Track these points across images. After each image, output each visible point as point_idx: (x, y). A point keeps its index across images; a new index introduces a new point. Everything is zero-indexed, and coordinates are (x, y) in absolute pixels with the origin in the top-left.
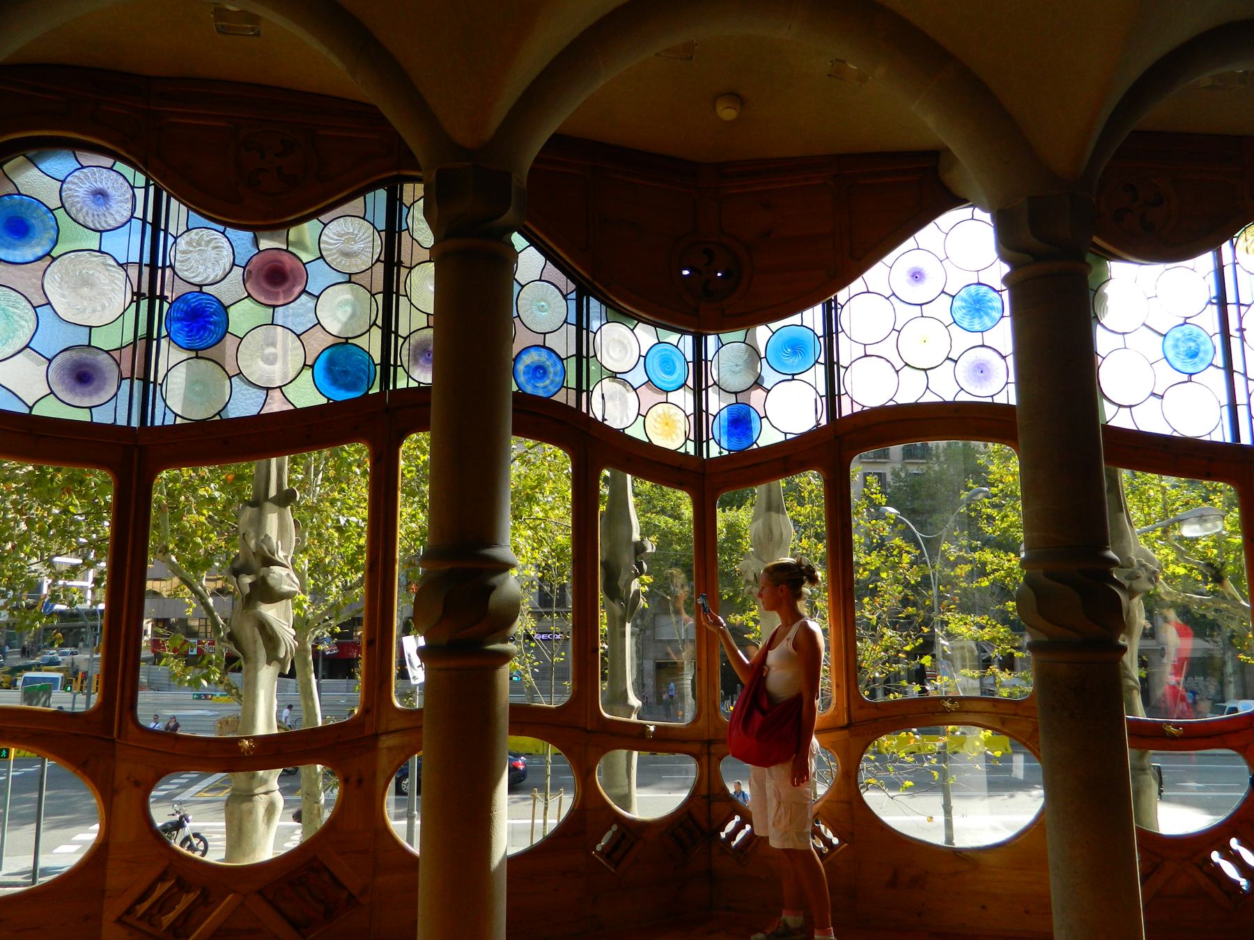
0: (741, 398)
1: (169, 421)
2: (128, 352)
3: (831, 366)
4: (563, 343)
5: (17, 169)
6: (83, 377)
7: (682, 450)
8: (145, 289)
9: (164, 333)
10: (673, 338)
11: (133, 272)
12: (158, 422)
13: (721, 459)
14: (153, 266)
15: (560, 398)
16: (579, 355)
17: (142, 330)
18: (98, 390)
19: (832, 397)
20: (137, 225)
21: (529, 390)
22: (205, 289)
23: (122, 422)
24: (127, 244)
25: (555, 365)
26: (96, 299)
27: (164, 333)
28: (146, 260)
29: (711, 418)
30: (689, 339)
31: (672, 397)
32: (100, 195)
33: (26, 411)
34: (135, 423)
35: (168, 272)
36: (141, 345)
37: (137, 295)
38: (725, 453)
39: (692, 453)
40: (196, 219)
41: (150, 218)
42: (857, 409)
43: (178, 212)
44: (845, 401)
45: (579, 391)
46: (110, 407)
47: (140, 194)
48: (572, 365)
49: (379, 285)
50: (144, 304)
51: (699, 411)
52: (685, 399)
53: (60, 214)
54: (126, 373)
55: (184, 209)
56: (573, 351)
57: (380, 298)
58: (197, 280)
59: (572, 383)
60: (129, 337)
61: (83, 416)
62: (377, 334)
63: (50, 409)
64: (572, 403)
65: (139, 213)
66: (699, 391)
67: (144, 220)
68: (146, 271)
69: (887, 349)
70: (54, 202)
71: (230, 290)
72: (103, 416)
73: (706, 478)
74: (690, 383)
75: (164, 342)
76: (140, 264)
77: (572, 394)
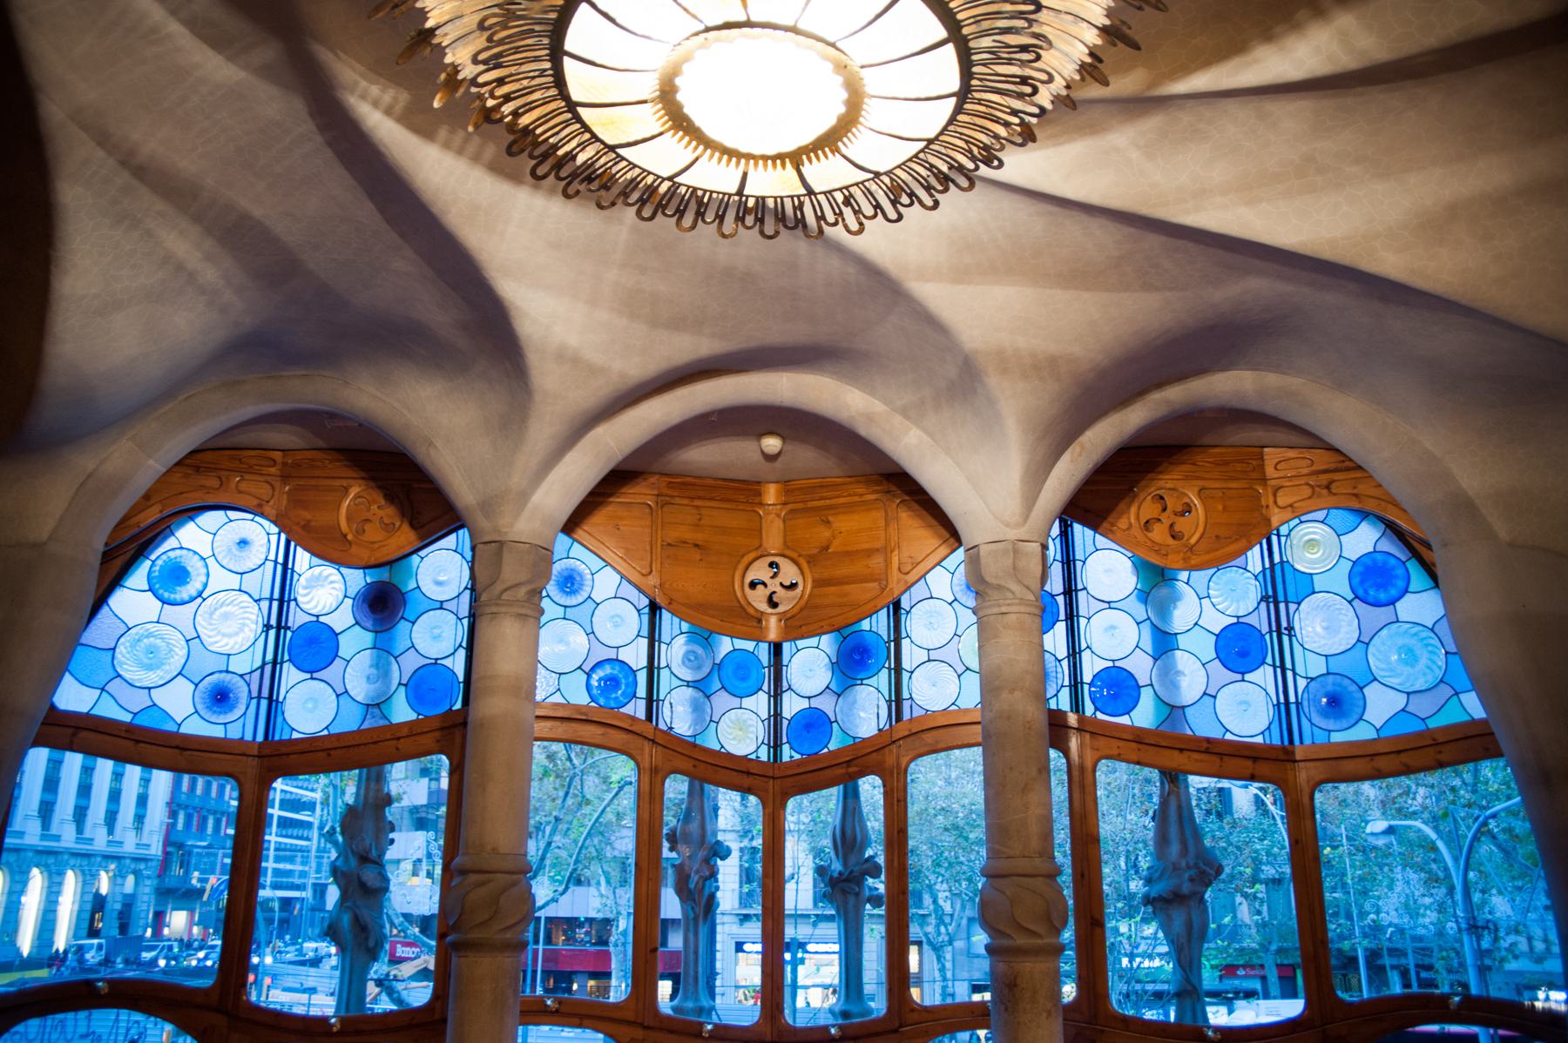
0: (815, 703)
1: (286, 737)
2: (257, 674)
3: (898, 669)
4: (636, 657)
5: (182, 524)
6: (221, 698)
7: (753, 757)
8: (273, 622)
9: (286, 657)
10: (749, 645)
11: (264, 605)
12: (277, 738)
13: (792, 763)
14: (281, 601)
15: (628, 710)
16: (652, 668)
17: (269, 657)
18: (232, 708)
19: (897, 701)
20: (270, 565)
21: (602, 701)
22: (322, 619)
23: (248, 737)
24: (263, 582)
25: (626, 677)
26: (234, 631)
27: (286, 657)
28: (276, 595)
29: (785, 723)
30: (764, 647)
31: (747, 702)
32: (243, 543)
33: (174, 729)
34: (260, 738)
35: (293, 604)
36: (268, 669)
37: (268, 627)
38: (797, 756)
39: (764, 758)
40: (316, 560)
41: (281, 560)
42: (917, 713)
43: (302, 558)
44: (906, 705)
45: (650, 700)
46: (239, 725)
47: (274, 539)
48: (642, 678)
49: (464, 610)
50: (272, 633)
51: (776, 715)
52: (760, 703)
53: (211, 562)
54: (255, 694)
55: (307, 555)
56: (644, 663)
57: (465, 622)
58: (315, 612)
59: (642, 691)
60: (258, 663)
61: (217, 732)
62: (462, 654)
63: (196, 727)
64: (641, 714)
65: (272, 556)
66: (777, 695)
67: (276, 562)
68: (275, 604)
69: (948, 654)
70: (206, 553)
71: (342, 619)
72: (234, 733)
73: (773, 783)
74: (765, 687)
75: (286, 666)
76: (271, 599)
77: (642, 705)
